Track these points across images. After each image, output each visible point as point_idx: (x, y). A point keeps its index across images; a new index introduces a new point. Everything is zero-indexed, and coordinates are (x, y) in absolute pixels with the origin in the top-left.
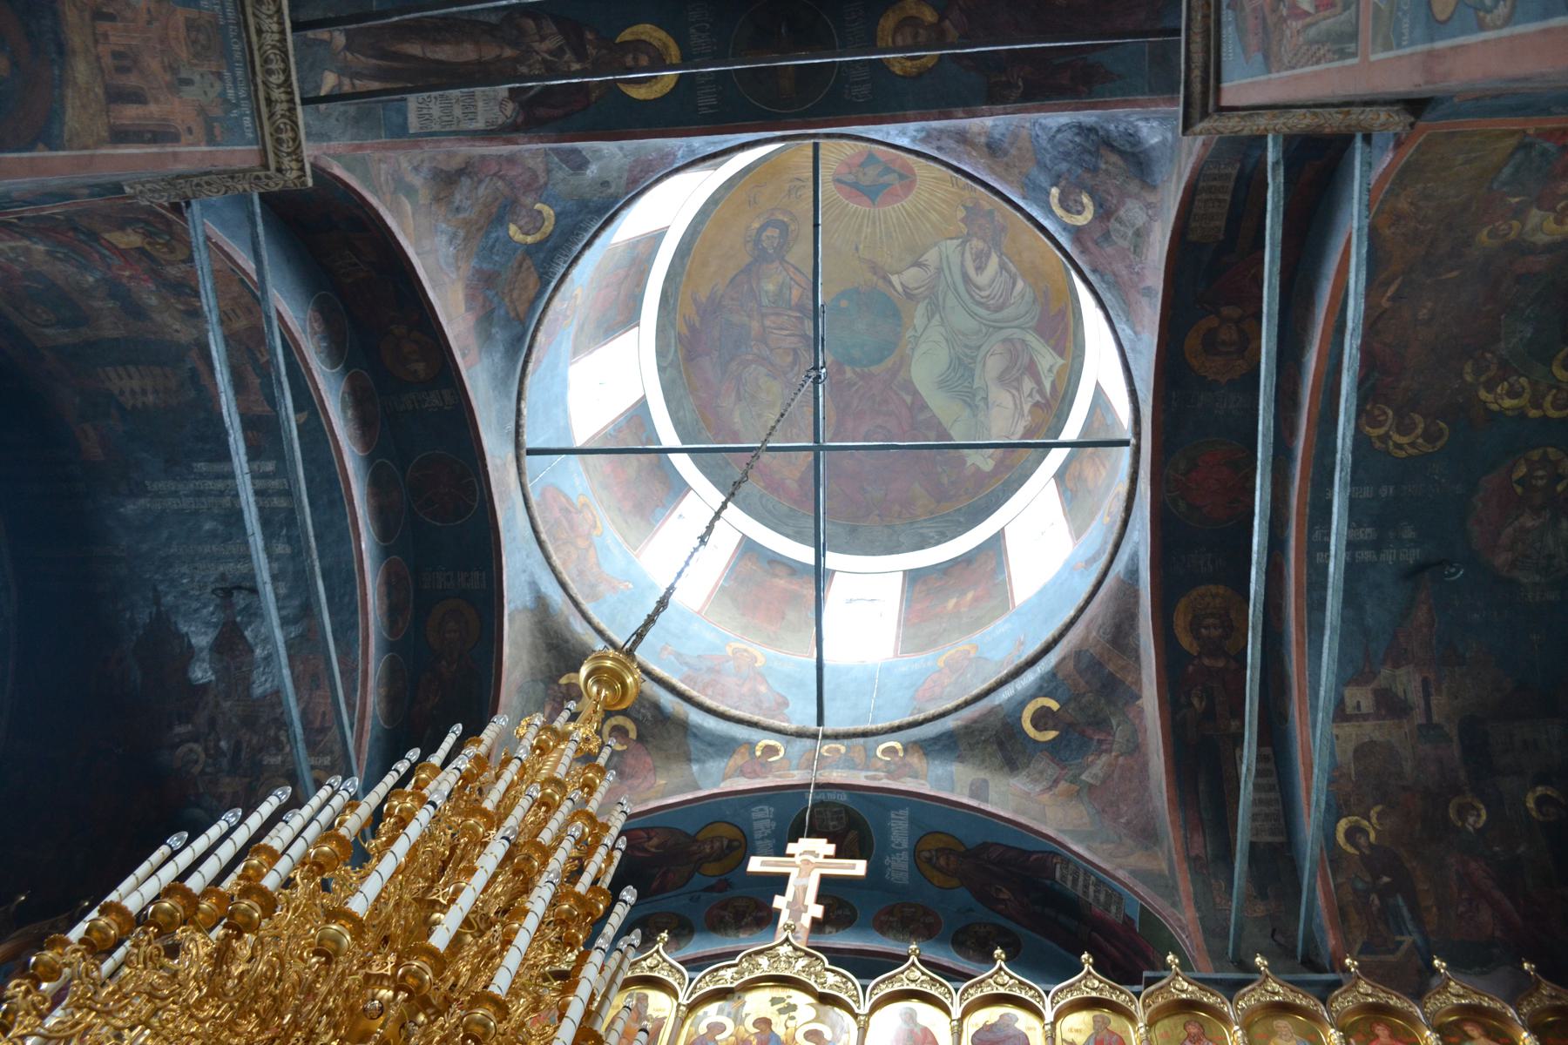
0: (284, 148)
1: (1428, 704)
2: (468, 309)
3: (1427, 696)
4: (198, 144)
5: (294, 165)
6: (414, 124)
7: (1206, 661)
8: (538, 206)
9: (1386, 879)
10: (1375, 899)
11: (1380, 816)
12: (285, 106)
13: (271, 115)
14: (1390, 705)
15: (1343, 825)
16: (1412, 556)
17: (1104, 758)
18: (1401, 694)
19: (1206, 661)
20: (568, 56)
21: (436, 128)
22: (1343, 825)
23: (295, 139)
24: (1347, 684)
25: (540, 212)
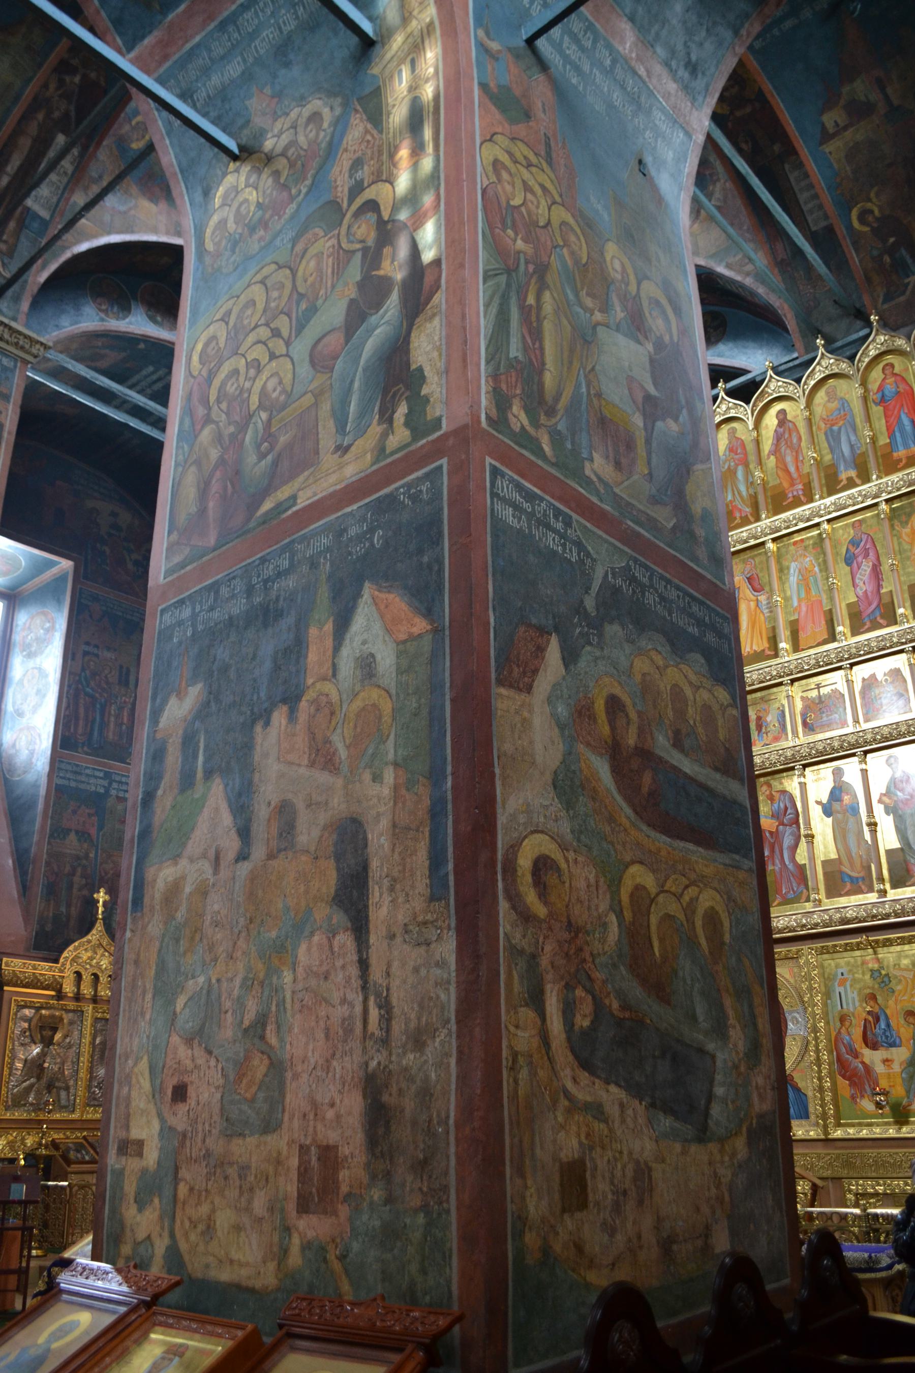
0: (27, 346)
1: (887, 97)
2: (156, 204)
3: (883, 89)
4: (7, 409)
5: (38, 346)
6: (45, 214)
7: (738, 114)
8: (134, 123)
9: (892, 240)
10: (887, 259)
11: (877, 195)
12: (6, 330)
13: (7, 342)
14: (859, 111)
15: (854, 213)
17: (718, 185)
18: (863, 98)
19: (738, 114)
20: (68, 79)
21: (55, 200)
22: (854, 213)
23: (26, 337)
24: (822, 113)
25: (138, 123)
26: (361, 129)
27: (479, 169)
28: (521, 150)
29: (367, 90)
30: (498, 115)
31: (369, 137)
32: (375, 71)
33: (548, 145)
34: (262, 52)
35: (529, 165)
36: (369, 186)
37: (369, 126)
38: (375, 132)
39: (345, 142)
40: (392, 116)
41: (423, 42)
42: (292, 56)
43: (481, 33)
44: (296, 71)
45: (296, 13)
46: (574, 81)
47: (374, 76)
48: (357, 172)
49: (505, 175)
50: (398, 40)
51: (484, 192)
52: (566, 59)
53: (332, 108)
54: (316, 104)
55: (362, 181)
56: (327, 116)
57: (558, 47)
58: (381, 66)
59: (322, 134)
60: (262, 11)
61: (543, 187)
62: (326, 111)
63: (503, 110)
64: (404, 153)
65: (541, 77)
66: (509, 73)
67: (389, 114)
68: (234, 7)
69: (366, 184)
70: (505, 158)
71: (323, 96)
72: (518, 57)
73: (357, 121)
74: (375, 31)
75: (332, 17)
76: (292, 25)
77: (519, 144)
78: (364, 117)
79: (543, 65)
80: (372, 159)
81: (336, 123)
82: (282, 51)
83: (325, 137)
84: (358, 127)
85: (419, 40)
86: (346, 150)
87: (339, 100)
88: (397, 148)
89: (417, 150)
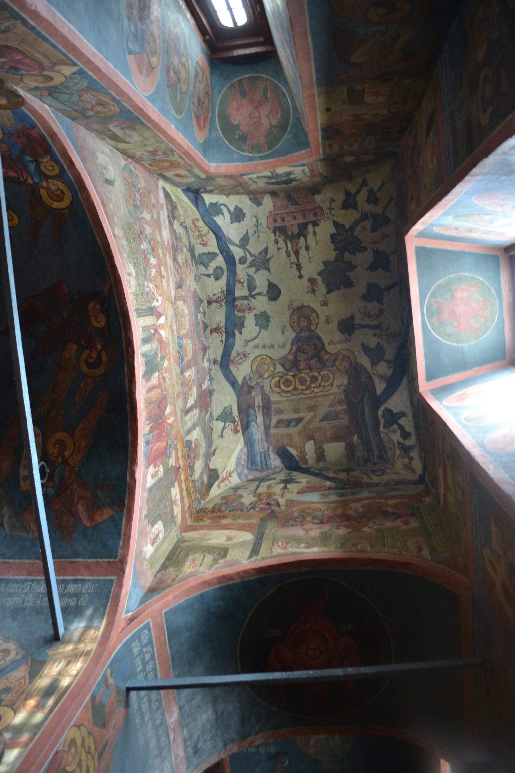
16: (273, 750)
26: (23, 674)
27: (63, 739)
28: (90, 742)
29: (40, 658)
30: (90, 716)
31: (23, 681)
32: (50, 652)
33: (104, 748)
34: (8, 604)
35: (88, 752)
36: (4, 706)
37: (27, 676)
38: (27, 681)
39: (10, 674)
40: (41, 680)
41: (80, 656)
42: (19, 617)
43: (109, 671)
44: (15, 624)
45: (36, 601)
46: (137, 721)
47: (47, 654)
48: (4, 693)
49: (73, 750)
50: (70, 647)
51: (57, 753)
52: (140, 708)
53: (17, 653)
54: (11, 646)
55: (3, 701)
56: (12, 655)
57: (140, 700)
58: (54, 652)
59: (3, 662)
60: (23, 589)
61: (88, 768)
62: (12, 655)
63: (95, 715)
64: (32, 702)
65: (123, 710)
66: (109, 698)
67: (41, 677)
68: (12, 577)
69: (3, 704)
70: (79, 741)
71: (18, 645)
72: (118, 693)
73: (23, 669)
74: (63, 635)
75: (49, 614)
76: (30, 604)
77: (91, 738)
78: (28, 670)
79: (127, 704)
80: (16, 693)
81: (13, 662)
82: (17, 612)
83: (3, 664)
84: (21, 672)
85: (79, 654)
86: (7, 679)
87: (24, 652)
88: (31, 697)
89: (39, 707)
